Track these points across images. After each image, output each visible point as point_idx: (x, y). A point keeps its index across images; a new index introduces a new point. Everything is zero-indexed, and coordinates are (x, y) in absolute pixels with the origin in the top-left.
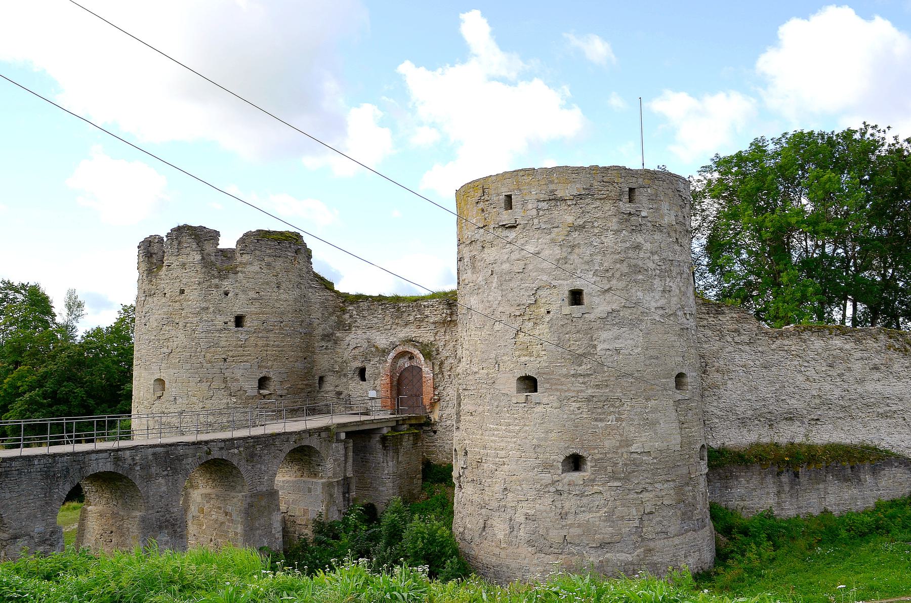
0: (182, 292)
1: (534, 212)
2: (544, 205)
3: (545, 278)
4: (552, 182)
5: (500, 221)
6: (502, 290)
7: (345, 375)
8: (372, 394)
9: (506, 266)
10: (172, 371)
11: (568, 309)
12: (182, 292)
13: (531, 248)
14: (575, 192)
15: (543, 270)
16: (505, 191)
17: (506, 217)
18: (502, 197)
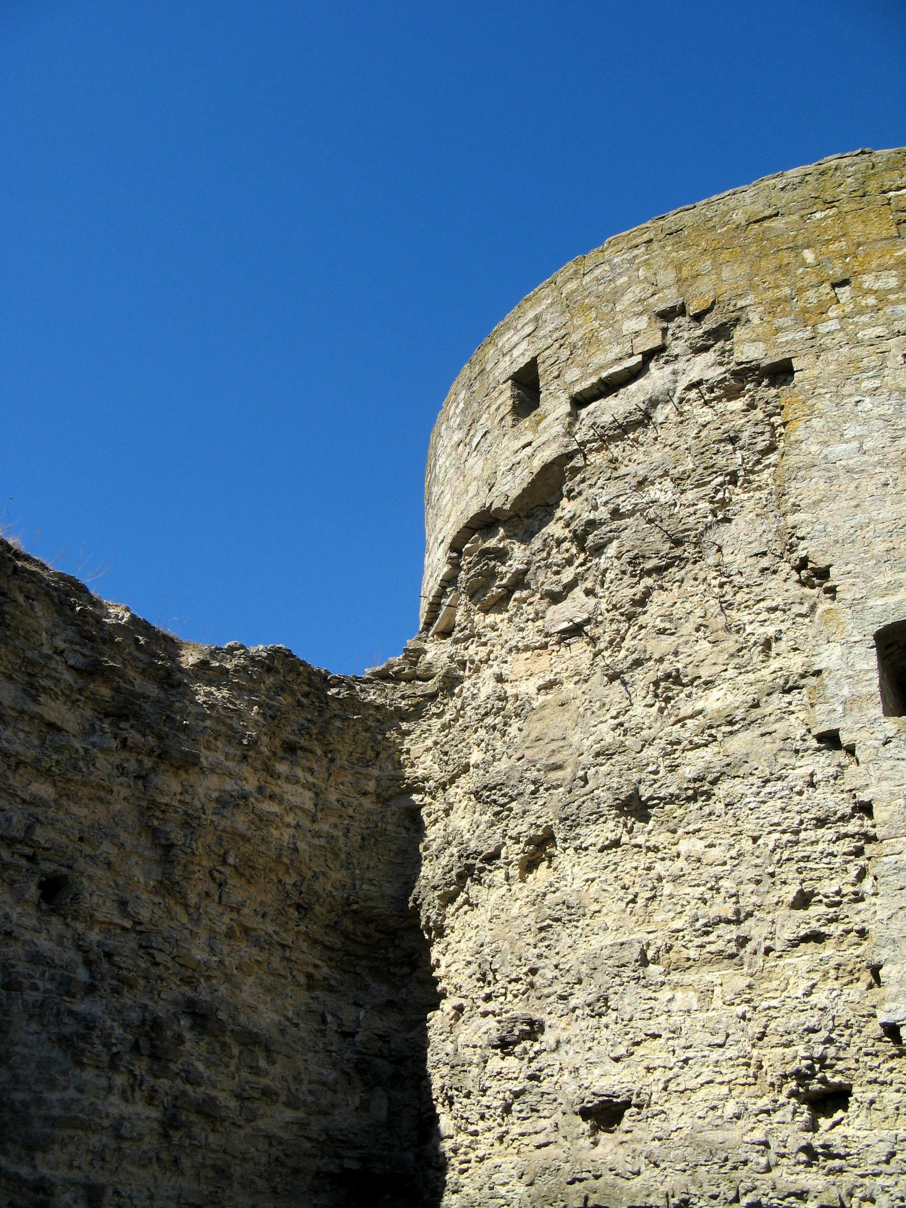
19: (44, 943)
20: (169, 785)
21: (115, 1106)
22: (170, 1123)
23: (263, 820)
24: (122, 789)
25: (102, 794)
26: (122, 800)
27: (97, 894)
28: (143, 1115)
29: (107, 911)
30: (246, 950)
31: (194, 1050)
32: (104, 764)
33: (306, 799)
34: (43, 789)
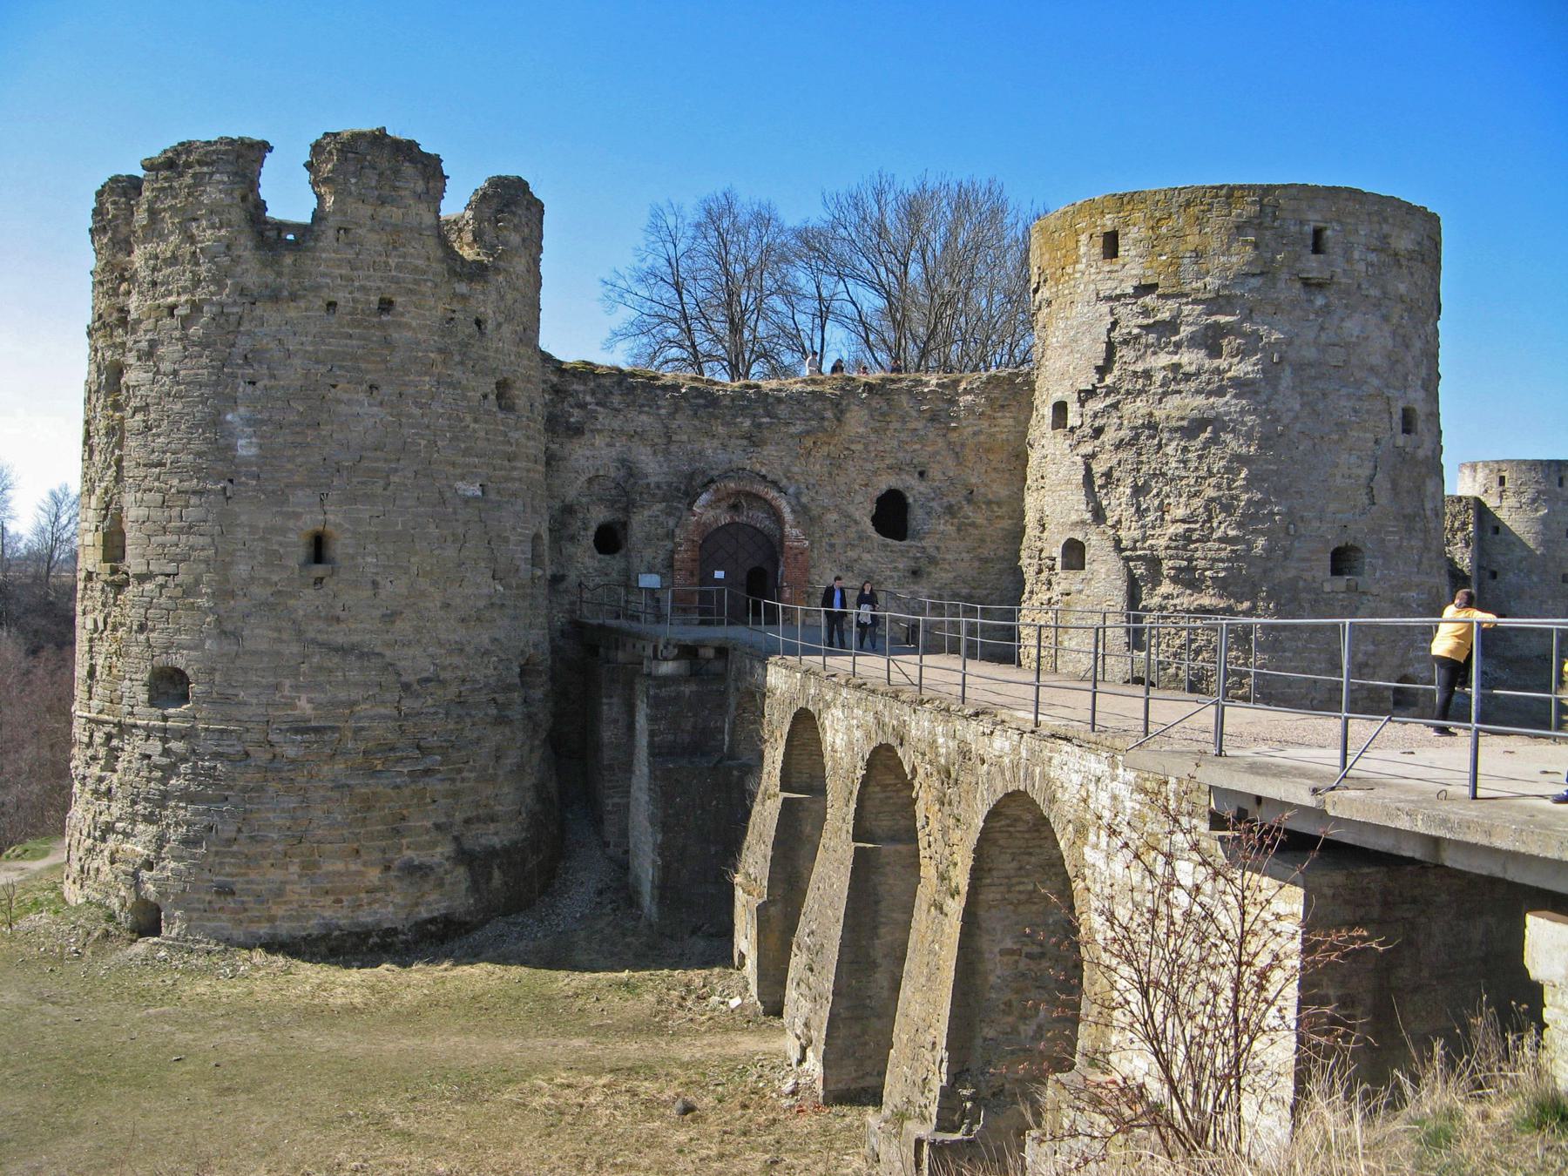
0: (386, 305)
1: (1362, 267)
2: (1373, 257)
3: (1375, 382)
4: (1385, 220)
5: (1303, 271)
6: (1302, 394)
7: (572, 538)
8: (650, 581)
9: (1310, 354)
10: (364, 511)
11: (1401, 440)
12: (386, 305)
13: (1352, 327)
14: (1411, 247)
15: (1372, 370)
16: (1314, 219)
17: (1313, 266)
18: (1308, 229)
19: (922, 489)
20: (953, 436)
21: (942, 527)
22: (959, 530)
23: (992, 435)
24: (940, 440)
25: (934, 443)
26: (941, 443)
27: (935, 472)
28: (951, 529)
29: (939, 476)
30: (994, 475)
31: (968, 510)
32: (931, 436)
33: (1011, 422)
34: (917, 446)
